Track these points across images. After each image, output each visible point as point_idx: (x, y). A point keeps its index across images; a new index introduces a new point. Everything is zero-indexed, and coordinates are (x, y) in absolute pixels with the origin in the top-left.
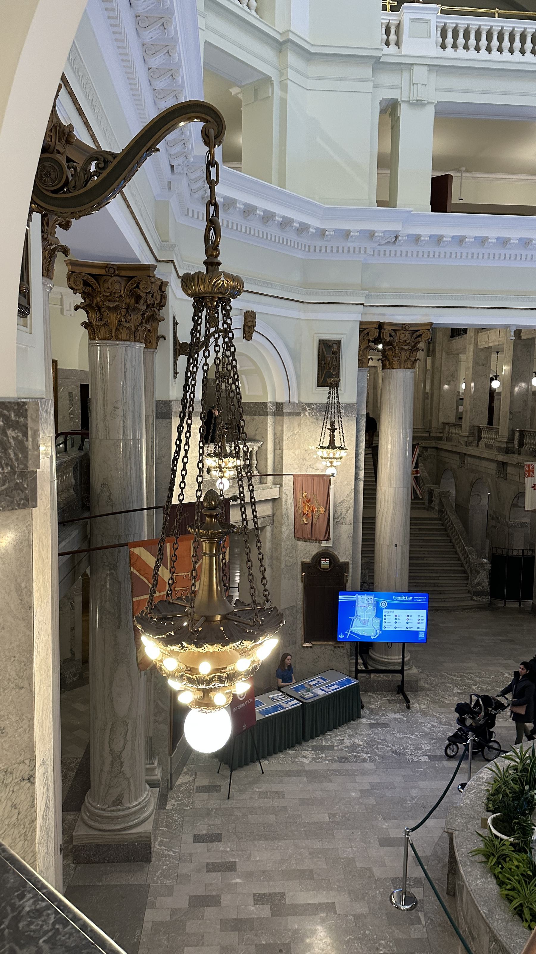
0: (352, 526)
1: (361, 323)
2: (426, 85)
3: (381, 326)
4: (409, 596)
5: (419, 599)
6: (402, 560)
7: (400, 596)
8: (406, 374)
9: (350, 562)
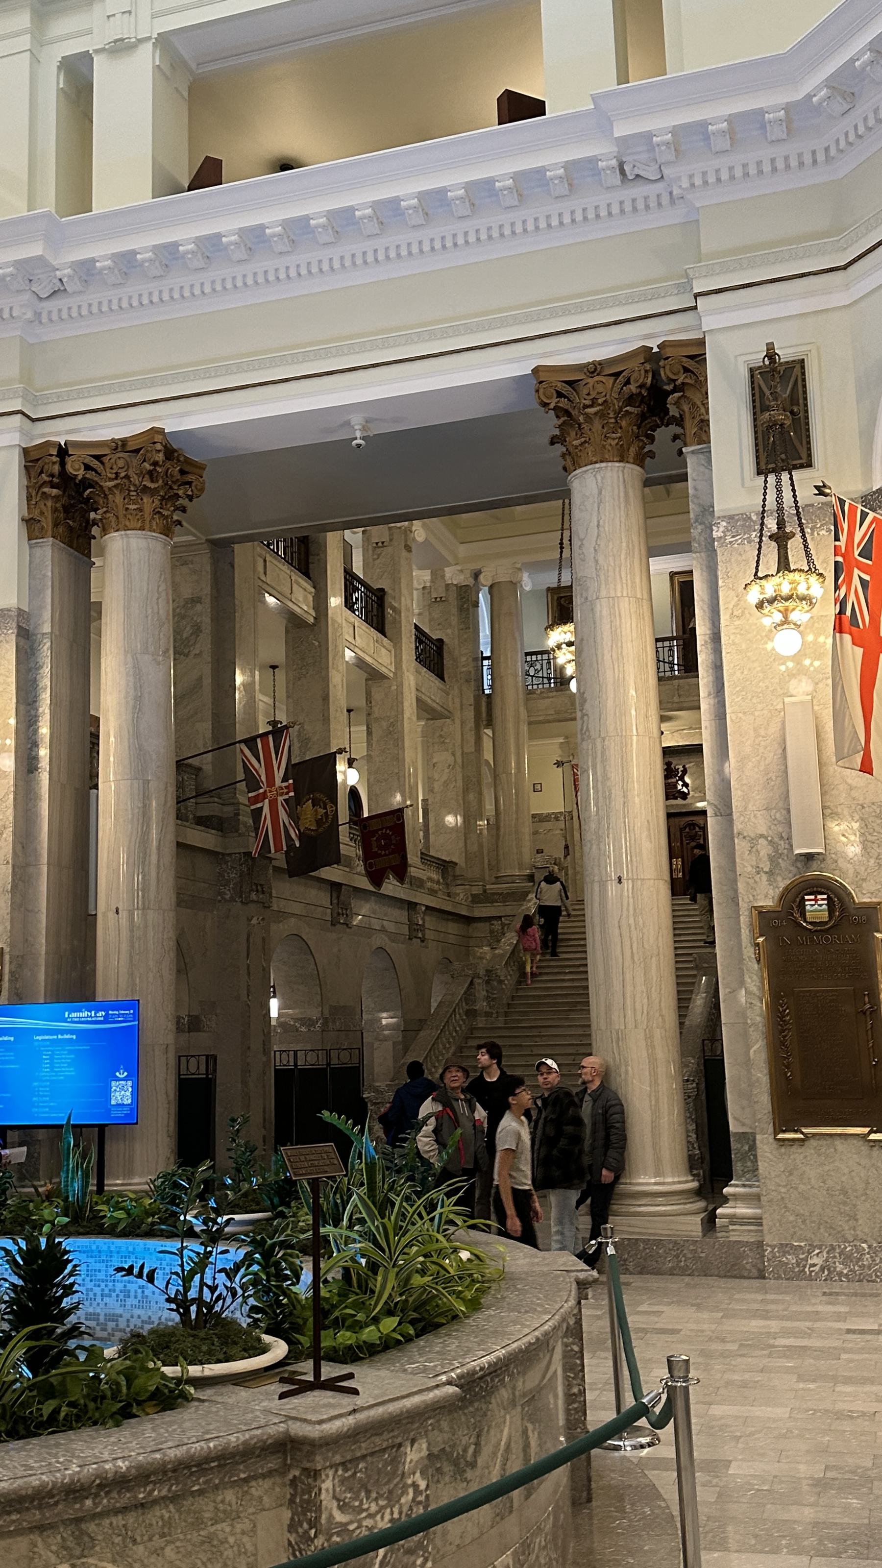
0: (10, 866)
1: (26, 451)
2: (130, 12)
3: (63, 452)
4: (97, 1011)
5: (119, 1016)
6: (132, 946)
7: (80, 1011)
8: (128, 543)
9: (7, 949)
